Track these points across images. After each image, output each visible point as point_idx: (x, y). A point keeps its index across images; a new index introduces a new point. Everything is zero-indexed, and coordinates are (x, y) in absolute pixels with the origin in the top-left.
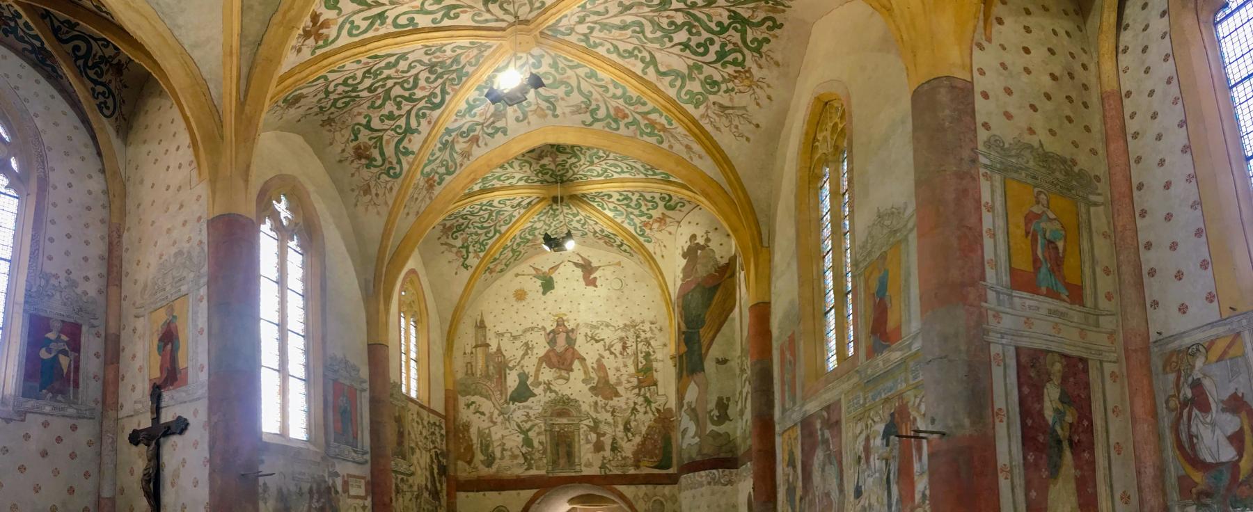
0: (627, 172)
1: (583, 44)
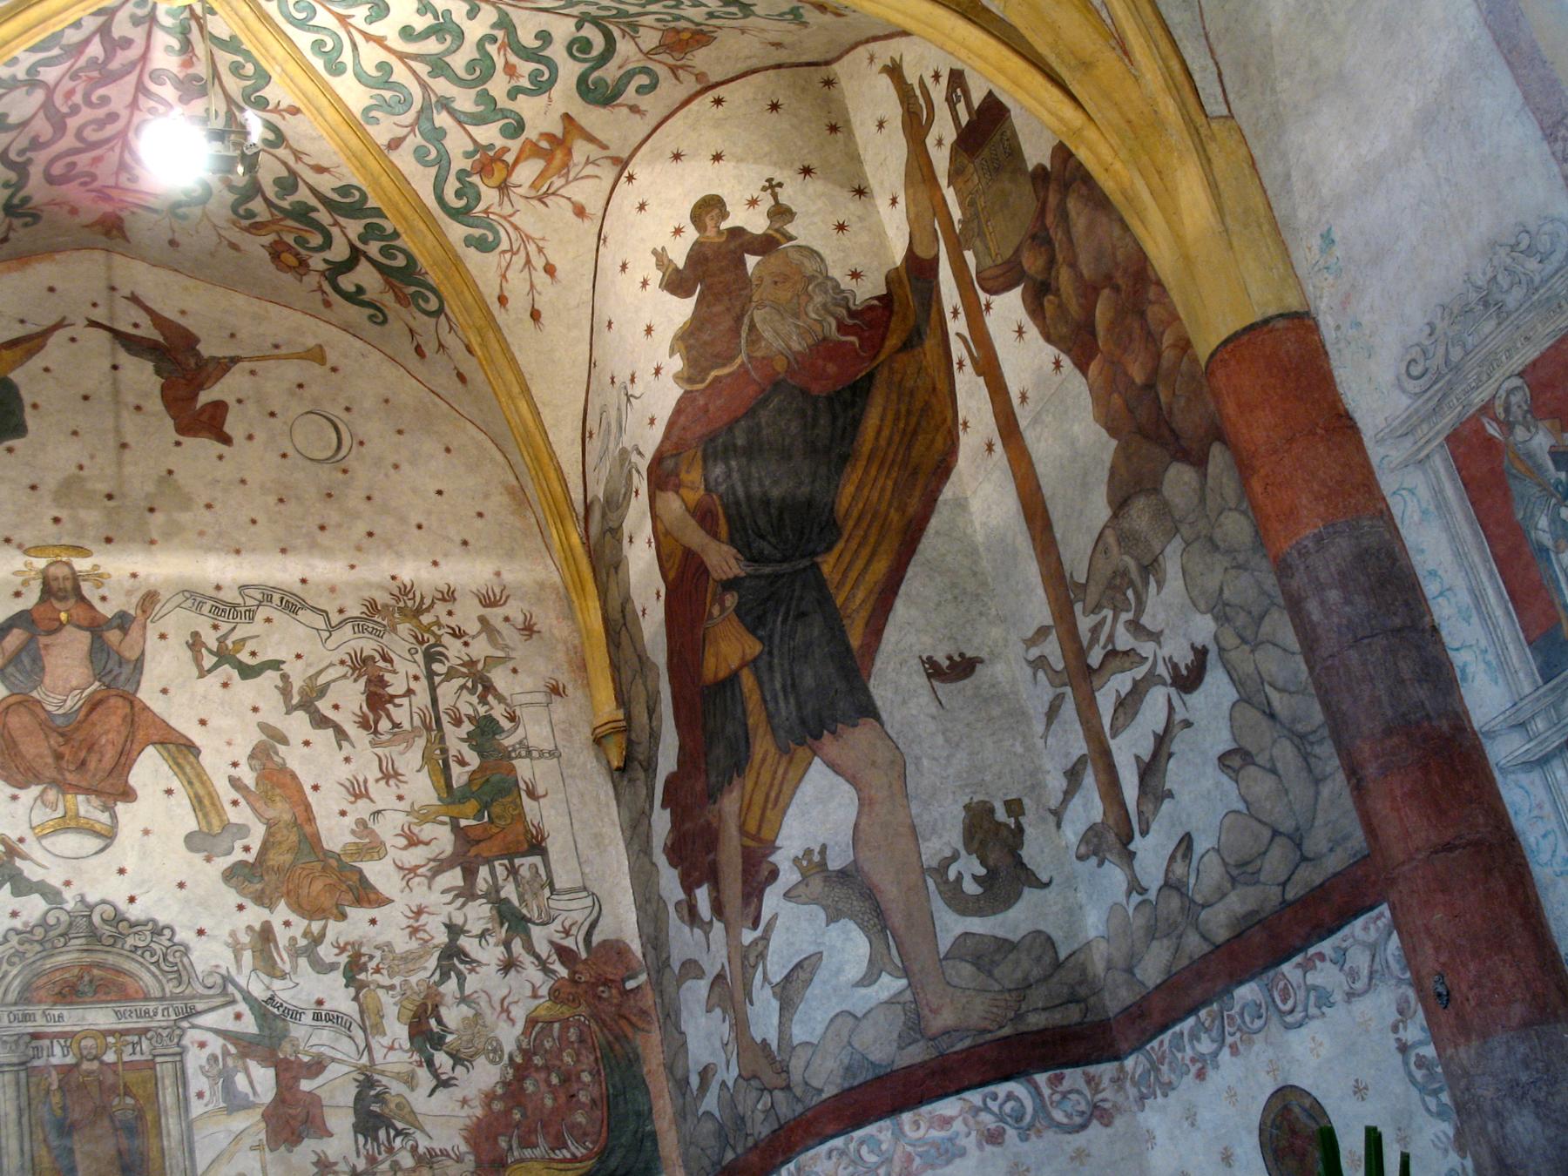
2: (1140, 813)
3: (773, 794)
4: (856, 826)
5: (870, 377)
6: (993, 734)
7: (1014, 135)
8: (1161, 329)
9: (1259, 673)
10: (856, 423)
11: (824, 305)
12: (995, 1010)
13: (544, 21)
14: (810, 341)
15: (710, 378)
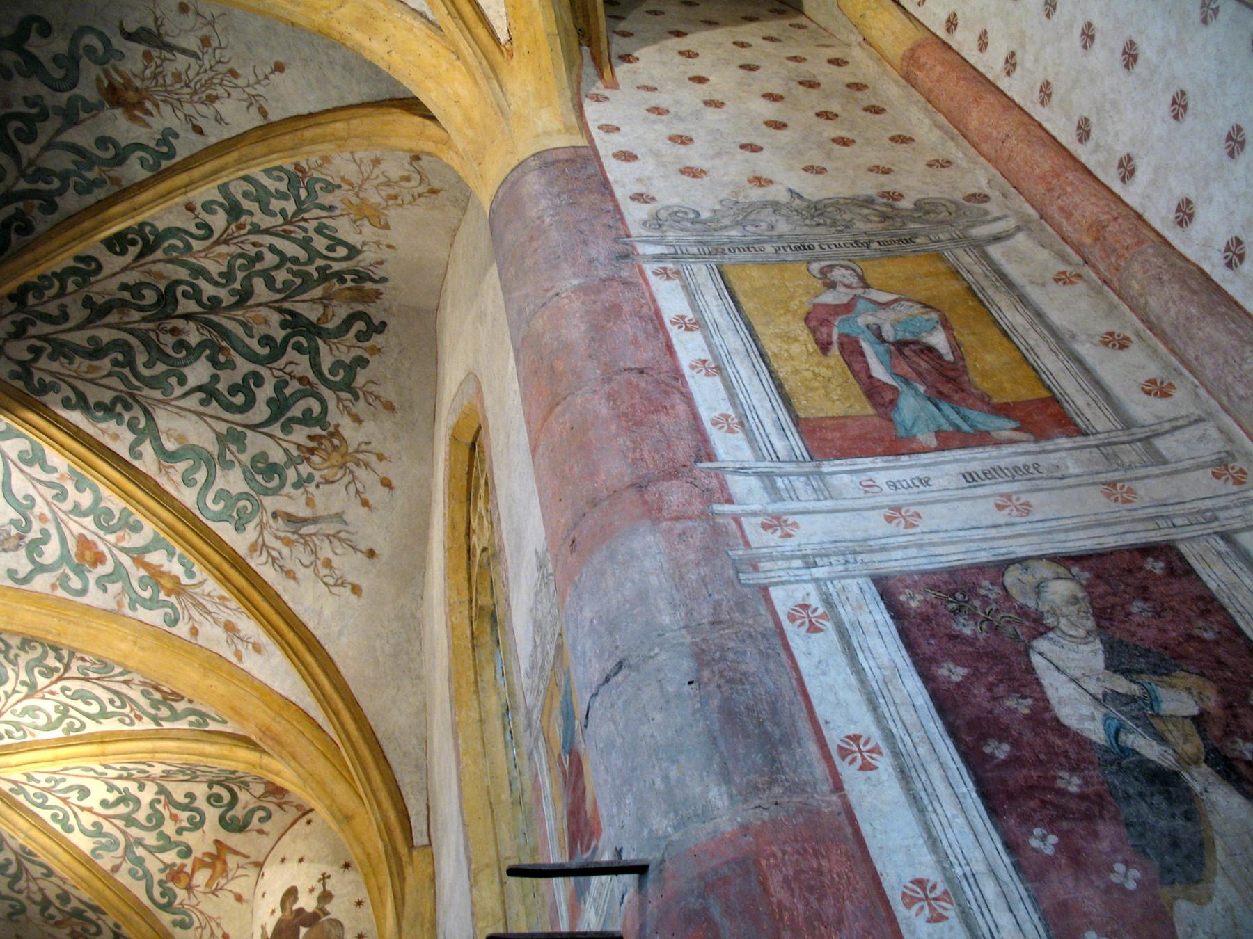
0: (113, 715)
1: (19, 384)
13: (188, 787)
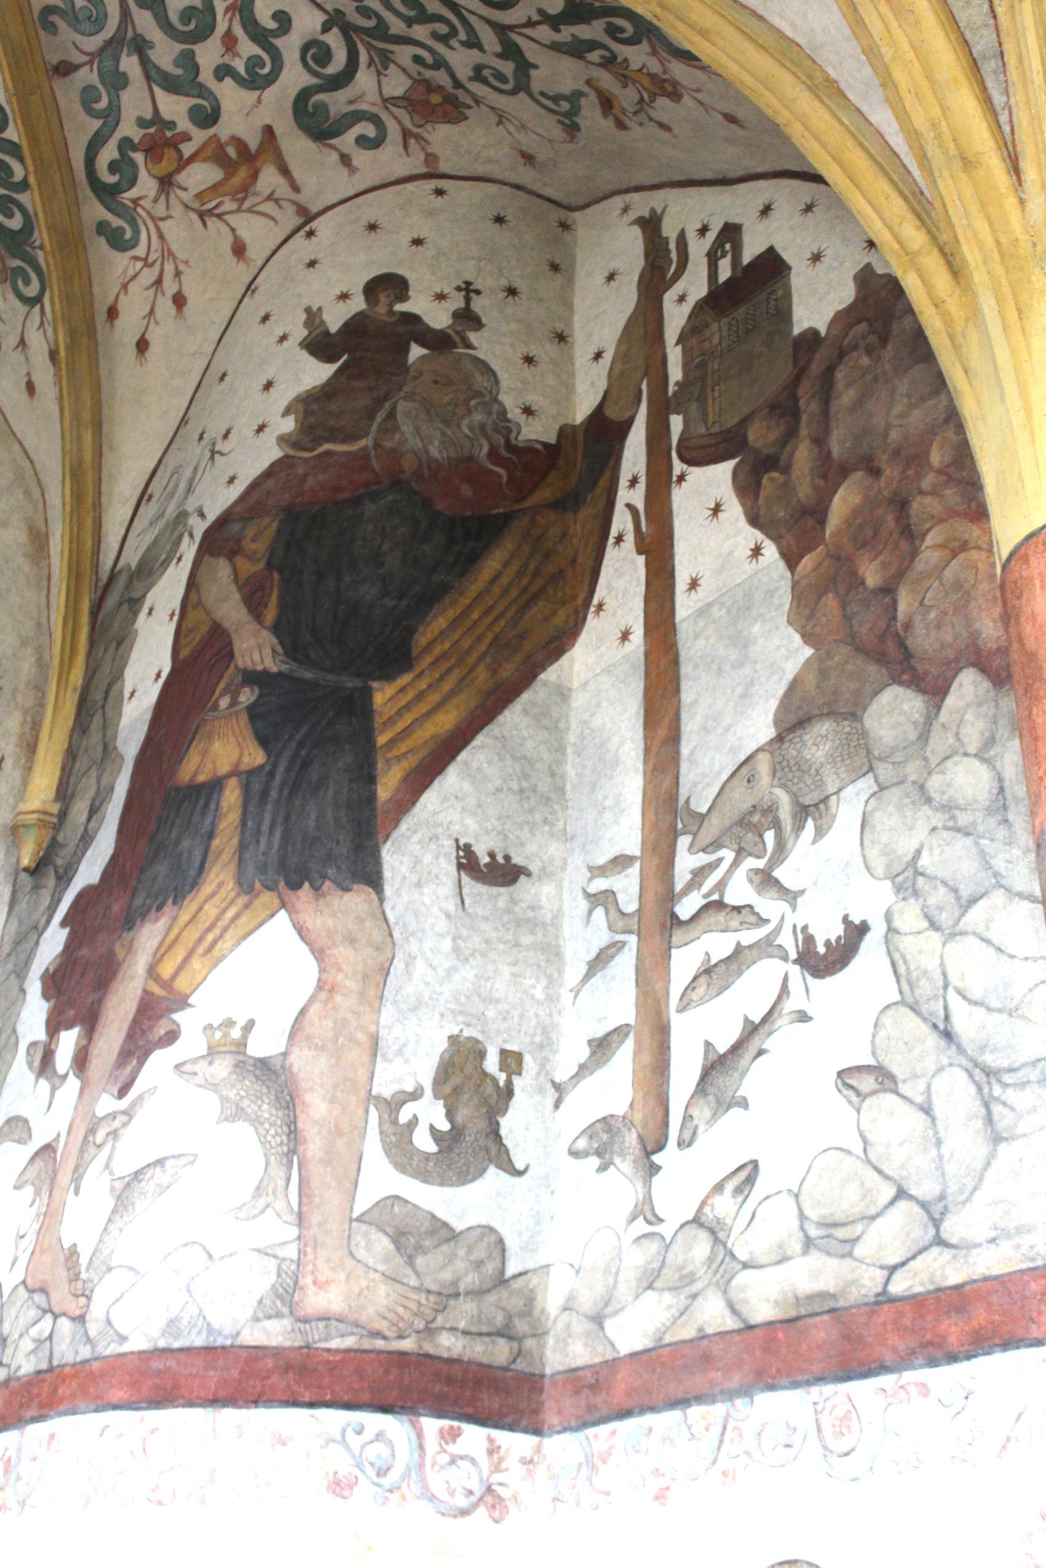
2: (687, 1117)
3: (210, 937)
4: (303, 1012)
5: (507, 518)
6: (515, 964)
7: (788, 295)
8: (928, 525)
9: (944, 975)
10: (470, 560)
11: (482, 426)
12: (401, 1310)
14: (452, 454)
15: (320, 450)
